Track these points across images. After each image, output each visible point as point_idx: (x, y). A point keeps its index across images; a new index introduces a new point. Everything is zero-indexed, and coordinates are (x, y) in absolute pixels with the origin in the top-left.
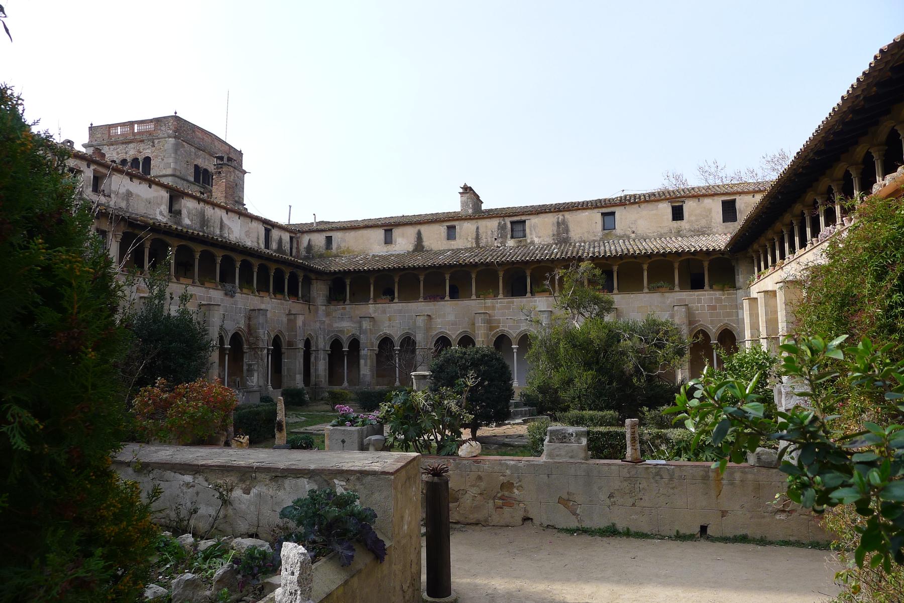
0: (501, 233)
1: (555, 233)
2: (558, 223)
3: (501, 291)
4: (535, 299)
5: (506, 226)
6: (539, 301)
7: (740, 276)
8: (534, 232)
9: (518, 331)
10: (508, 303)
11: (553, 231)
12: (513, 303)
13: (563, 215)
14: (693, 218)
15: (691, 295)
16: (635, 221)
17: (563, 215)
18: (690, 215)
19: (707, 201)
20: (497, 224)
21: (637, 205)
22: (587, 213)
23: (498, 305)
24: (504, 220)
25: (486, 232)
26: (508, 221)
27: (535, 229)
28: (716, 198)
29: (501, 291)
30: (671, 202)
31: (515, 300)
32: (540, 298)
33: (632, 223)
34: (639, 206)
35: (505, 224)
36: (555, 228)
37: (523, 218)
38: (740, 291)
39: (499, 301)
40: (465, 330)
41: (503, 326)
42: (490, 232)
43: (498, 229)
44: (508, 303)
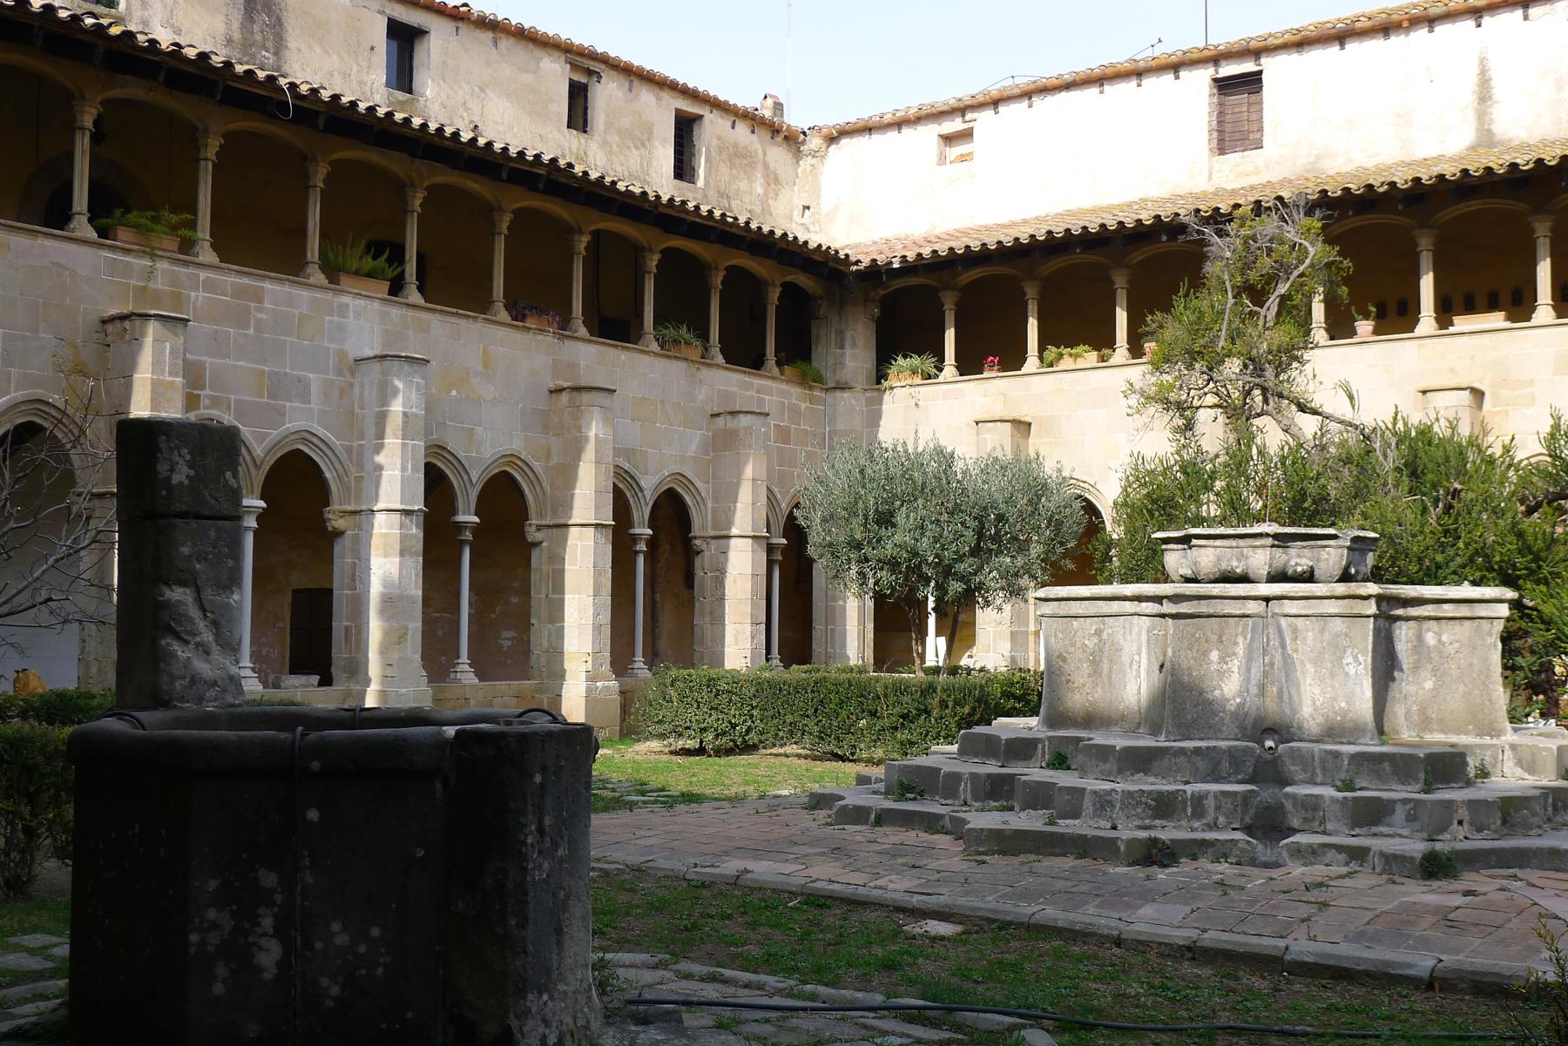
4: (346, 299)
6: (357, 315)
7: (848, 351)
9: (275, 434)
10: (240, 293)
12: (260, 300)
19: (647, 96)
23: (198, 297)
30: (575, 67)
31: (267, 285)
32: (362, 302)
34: (496, 43)
38: (846, 395)
39: (203, 275)
40: (39, 393)
41: (216, 401)
44: (240, 293)
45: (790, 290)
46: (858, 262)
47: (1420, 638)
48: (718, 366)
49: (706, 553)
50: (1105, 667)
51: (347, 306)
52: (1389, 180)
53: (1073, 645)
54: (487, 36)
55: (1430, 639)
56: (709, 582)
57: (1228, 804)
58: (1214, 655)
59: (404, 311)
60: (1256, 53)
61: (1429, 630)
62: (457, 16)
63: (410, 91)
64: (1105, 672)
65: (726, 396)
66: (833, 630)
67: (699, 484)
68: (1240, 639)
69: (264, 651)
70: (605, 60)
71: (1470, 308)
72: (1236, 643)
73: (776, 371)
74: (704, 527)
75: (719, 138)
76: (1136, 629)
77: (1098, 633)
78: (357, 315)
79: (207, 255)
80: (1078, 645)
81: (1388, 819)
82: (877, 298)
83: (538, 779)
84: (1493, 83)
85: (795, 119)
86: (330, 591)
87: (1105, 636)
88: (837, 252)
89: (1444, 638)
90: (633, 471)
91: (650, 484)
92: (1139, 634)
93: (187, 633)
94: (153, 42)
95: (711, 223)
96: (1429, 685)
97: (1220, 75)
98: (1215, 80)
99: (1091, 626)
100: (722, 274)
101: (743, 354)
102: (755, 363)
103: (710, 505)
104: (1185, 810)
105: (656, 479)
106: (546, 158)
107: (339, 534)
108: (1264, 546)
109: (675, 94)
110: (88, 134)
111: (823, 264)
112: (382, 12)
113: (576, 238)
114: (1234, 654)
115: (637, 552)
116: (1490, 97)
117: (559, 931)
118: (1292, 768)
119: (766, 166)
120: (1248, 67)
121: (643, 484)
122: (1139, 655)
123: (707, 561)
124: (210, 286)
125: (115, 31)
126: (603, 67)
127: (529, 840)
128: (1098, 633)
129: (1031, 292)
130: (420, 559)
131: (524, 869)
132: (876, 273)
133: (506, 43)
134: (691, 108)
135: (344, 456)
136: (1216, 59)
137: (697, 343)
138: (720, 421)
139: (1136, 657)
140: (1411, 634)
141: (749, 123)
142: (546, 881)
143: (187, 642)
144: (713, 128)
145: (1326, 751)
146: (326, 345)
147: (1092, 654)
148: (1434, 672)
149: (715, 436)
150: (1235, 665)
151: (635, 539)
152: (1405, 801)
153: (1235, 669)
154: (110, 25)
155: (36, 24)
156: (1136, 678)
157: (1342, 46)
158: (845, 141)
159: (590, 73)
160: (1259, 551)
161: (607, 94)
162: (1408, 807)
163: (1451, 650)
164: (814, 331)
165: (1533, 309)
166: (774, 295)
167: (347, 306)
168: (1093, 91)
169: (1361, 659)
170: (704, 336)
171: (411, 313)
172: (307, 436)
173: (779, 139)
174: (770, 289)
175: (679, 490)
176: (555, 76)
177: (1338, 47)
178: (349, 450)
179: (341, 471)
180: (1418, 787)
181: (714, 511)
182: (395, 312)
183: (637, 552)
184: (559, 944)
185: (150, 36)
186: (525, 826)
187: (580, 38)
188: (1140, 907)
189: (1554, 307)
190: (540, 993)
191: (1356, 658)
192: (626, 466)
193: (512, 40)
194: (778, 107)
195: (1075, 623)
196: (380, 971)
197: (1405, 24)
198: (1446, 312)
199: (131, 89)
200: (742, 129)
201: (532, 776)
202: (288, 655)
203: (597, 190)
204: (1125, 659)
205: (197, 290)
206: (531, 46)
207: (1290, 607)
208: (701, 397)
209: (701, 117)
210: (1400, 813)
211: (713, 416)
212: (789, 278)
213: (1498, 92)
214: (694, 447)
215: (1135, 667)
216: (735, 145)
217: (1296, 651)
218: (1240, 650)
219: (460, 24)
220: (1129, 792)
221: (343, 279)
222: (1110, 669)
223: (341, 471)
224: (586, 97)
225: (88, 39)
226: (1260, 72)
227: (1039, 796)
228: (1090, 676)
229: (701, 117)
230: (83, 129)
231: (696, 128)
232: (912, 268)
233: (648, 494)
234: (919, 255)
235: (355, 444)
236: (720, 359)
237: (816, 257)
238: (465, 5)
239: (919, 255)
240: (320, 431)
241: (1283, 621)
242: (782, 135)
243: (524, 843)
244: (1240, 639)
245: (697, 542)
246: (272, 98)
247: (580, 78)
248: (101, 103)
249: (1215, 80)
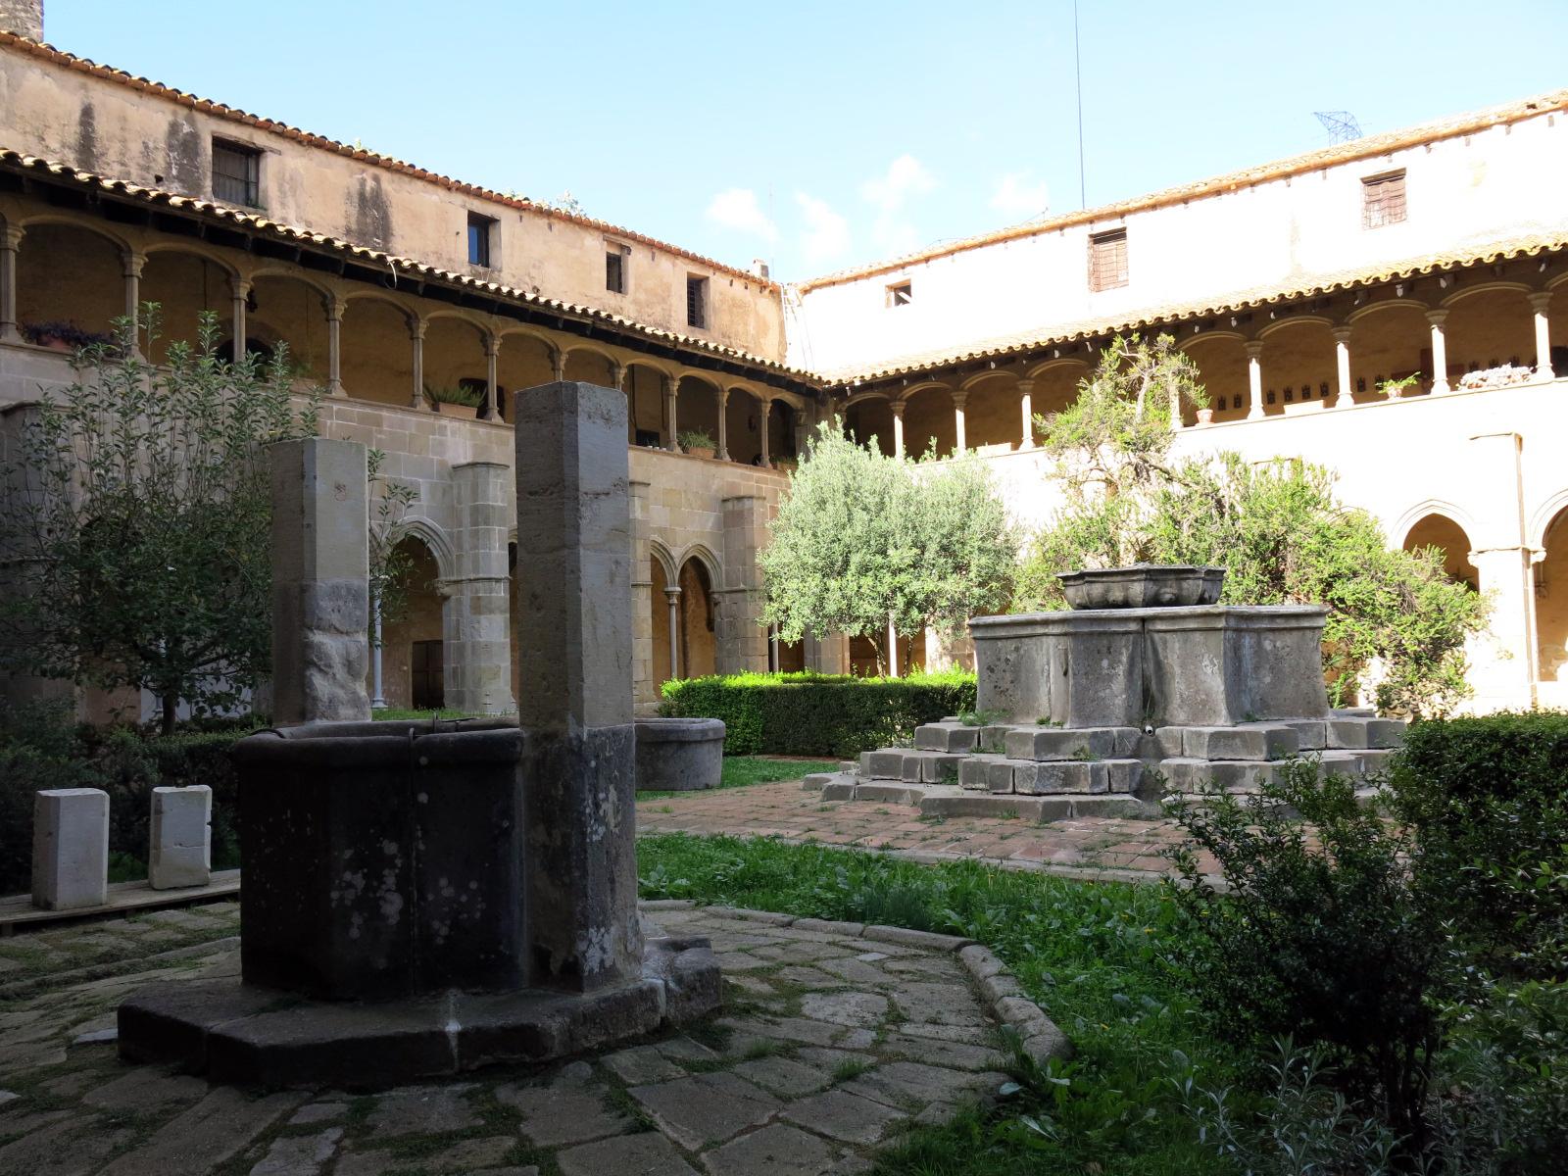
0: (181, 166)
1: (354, 227)
2: (362, 196)
3: (336, 375)
4: (444, 422)
5: (196, 145)
6: (454, 434)
8: (290, 201)
10: (363, 419)
11: (347, 217)
12: (379, 425)
13: (376, 179)
14: (642, 297)
15: (749, 478)
16: (540, 262)
17: (376, 179)
18: (638, 286)
19: (665, 263)
20: (165, 127)
21: (545, 221)
22: (435, 198)
24: (191, 122)
25: (124, 141)
26: (208, 128)
27: (294, 195)
28: (680, 262)
29: (336, 375)
30: (610, 243)
31: (385, 413)
32: (456, 424)
33: (534, 266)
34: (550, 227)
35: (194, 137)
36: (354, 211)
37: (260, 139)
39: (335, 407)
42: (135, 148)
43: (171, 147)
45: (778, 405)
46: (829, 382)
47: (1259, 644)
48: (726, 463)
49: (722, 604)
51: (446, 427)
52: (1224, 305)
53: (999, 660)
54: (543, 222)
55: (1268, 645)
56: (725, 627)
57: (1117, 775)
58: (1105, 663)
59: (489, 430)
60: (1122, 215)
61: (1265, 639)
62: (520, 207)
63: (487, 265)
64: (1023, 679)
65: (733, 485)
66: (819, 659)
67: (715, 553)
68: (1124, 651)
69: (393, 689)
70: (633, 237)
71: (1289, 398)
72: (1121, 654)
73: (770, 465)
74: (720, 585)
75: (721, 294)
76: (1045, 646)
77: (1017, 649)
78: (454, 434)
79: (339, 392)
80: (1003, 659)
81: (1240, 781)
82: (844, 409)
83: (593, 764)
85: (775, 278)
86: (440, 642)
87: (1022, 652)
88: (812, 375)
89: (1278, 644)
90: (666, 545)
91: (679, 553)
92: (1048, 650)
93: (326, 666)
94: (290, 232)
95: (717, 357)
96: (1268, 680)
97: (1095, 232)
98: (1091, 236)
99: (1011, 645)
100: (726, 395)
101: (747, 454)
102: (755, 460)
103: (724, 568)
104: (1086, 779)
105: (682, 550)
106: (591, 311)
107: (446, 598)
108: (1140, 580)
109: (687, 261)
110: (243, 303)
111: (803, 385)
112: (464, 206)
113: (616, 370)
114: (1120, 661)
115: (671, 605)
117: (612, 881)
118: (1167, 745)
119: (757, 313)
120: (1115, 224)
121: (673, 553)
122: (1048, 664)
123: (723, 611)
124: (340, 415)
125: (261, 224)
126: (632, 242)
127: (588, 811)
128: (1017, 649)
129: (960, 397)
130: (508, 615)
131: (584, 834)
132: (840, 390)
133: (558, 226)
134: (698, 271)
135: (447, 539)
136: (1091, 221)
137: (711, 445)
138: (730, 505)
140: (1252, 641)
141: (743, 281)
142: (601, 842)
143: (326, 673)
144: (718, 288)
145: (1192, 732)
146: (431, 456)
148: (1272, 668)
149: (725, 516)
150: (1121, 670)
151: (669, 595)
152: (1252, 767)
153: (1121, 673)
154: (256, 220)
155: (200, 220)
158: (815, 292)
159: (622, 247)
160: (1136, 584)
161: (636, 263)
162: (1255, 771)
163: (1283, 653)
164: (797, 435)
165: (1337, 397)
166: (767, 408)
167: (446, 427)
168: (1001, 245)
170: (715, 438)
171: (494, 431)
172: (419, 525)
173: (767, 292)
174: (763, 404)
175: (700, 557)
176: (596, 251)
178: (451, 535)
179: (446, 552)
180: (1263, 756)
181: (727, 573)
182: (482, 431)
183: (671, 605)
184: (613, 890)
185: (287, 227)
186: (584, 800)
187: (613, 222)
188: (1056, 851)
189: (1352, 395)
190: (598, 928)
191: (1212, 662)
192: (660, 540)
193: (563, 224)
194: (765, 269)
195: (1000, 644)
196: (478, 915)
197: (1233, 187)
198: (1274, 402)
199: (274, 268)
200: (738, 284)
201: (587, 763)
202: (411, 690)
203: (631, 334)
204: (1038, 668)
205: (331, 418)
206: (577, 227)
207: (1160, 626)
208: (714, 487)
209: (708, 278)
211: (725, 501)
212: (778, 396)
214: (710, 524)
216: (733, 299)
217: (1166, 657)
218: (1124, 659)
219: (524, 214)
220: (1044, 767)
221: (442, 406)
223: (446, 552)
224: (620, 266)
225: (241, 231)
226: (1124, 229)
227: (976, 773)
228: (1012, 682)
229: (708, 278)
230: (239, 299)
231: (703, 286)
232: (868, 385)
233: (677, 561)
234: (874, 375)
235: (455, 530)
236: (727, 458)
237: (797, 380)
238: (526, 199)
239: (874, 375)
240: (429, 522)
241: (1156, 636)
242: (768, 290)
243: (584, 813)
244: (1124, 651)
245: (716, 596)
246: (381, 272)
247: (615, 251)
248: (253, 279)
249: (1091, 236)
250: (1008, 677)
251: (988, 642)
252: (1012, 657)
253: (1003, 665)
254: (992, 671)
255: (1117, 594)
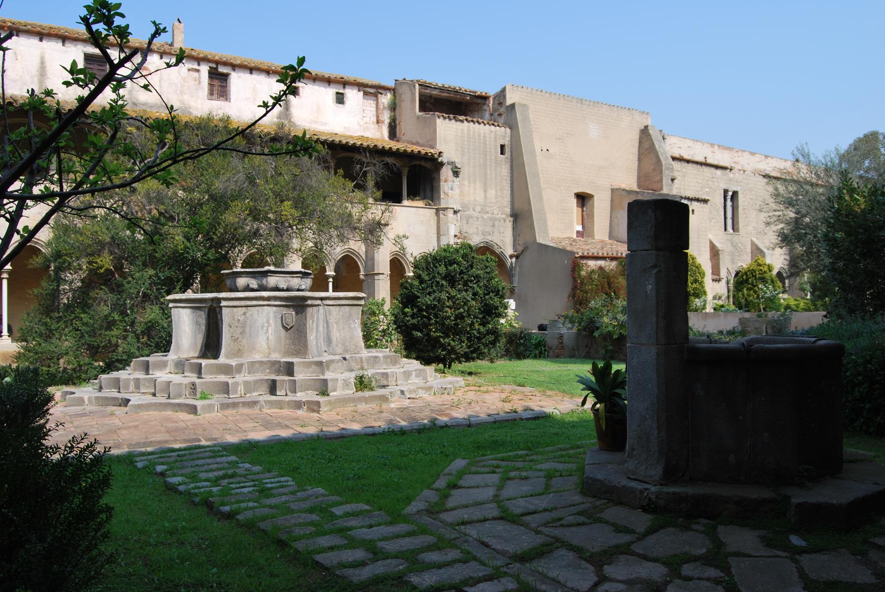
50: (248, 329)
77: (244, 314)
84: (48, 69)
87: (248, 315)
108: (297, 277)
116: (46, 75)
128: (244, 314)
139: (266, 324)
147: (242, 324)
156: (266, 333)
157: (41, 40)
160: (295, 279)
169: (356, 321)
177: (61, 44)
195: (235, 309)
210: (414, 373)
213: (49, 74)
215: (265, 328)
217: (330, 319)
222: (250, 331)
228: (241, 333)
250: (239, 330)
251: (229, 308)
252: (242, 318)
253: (236, 324)
254: (231, 327)
255: (283, 285)
